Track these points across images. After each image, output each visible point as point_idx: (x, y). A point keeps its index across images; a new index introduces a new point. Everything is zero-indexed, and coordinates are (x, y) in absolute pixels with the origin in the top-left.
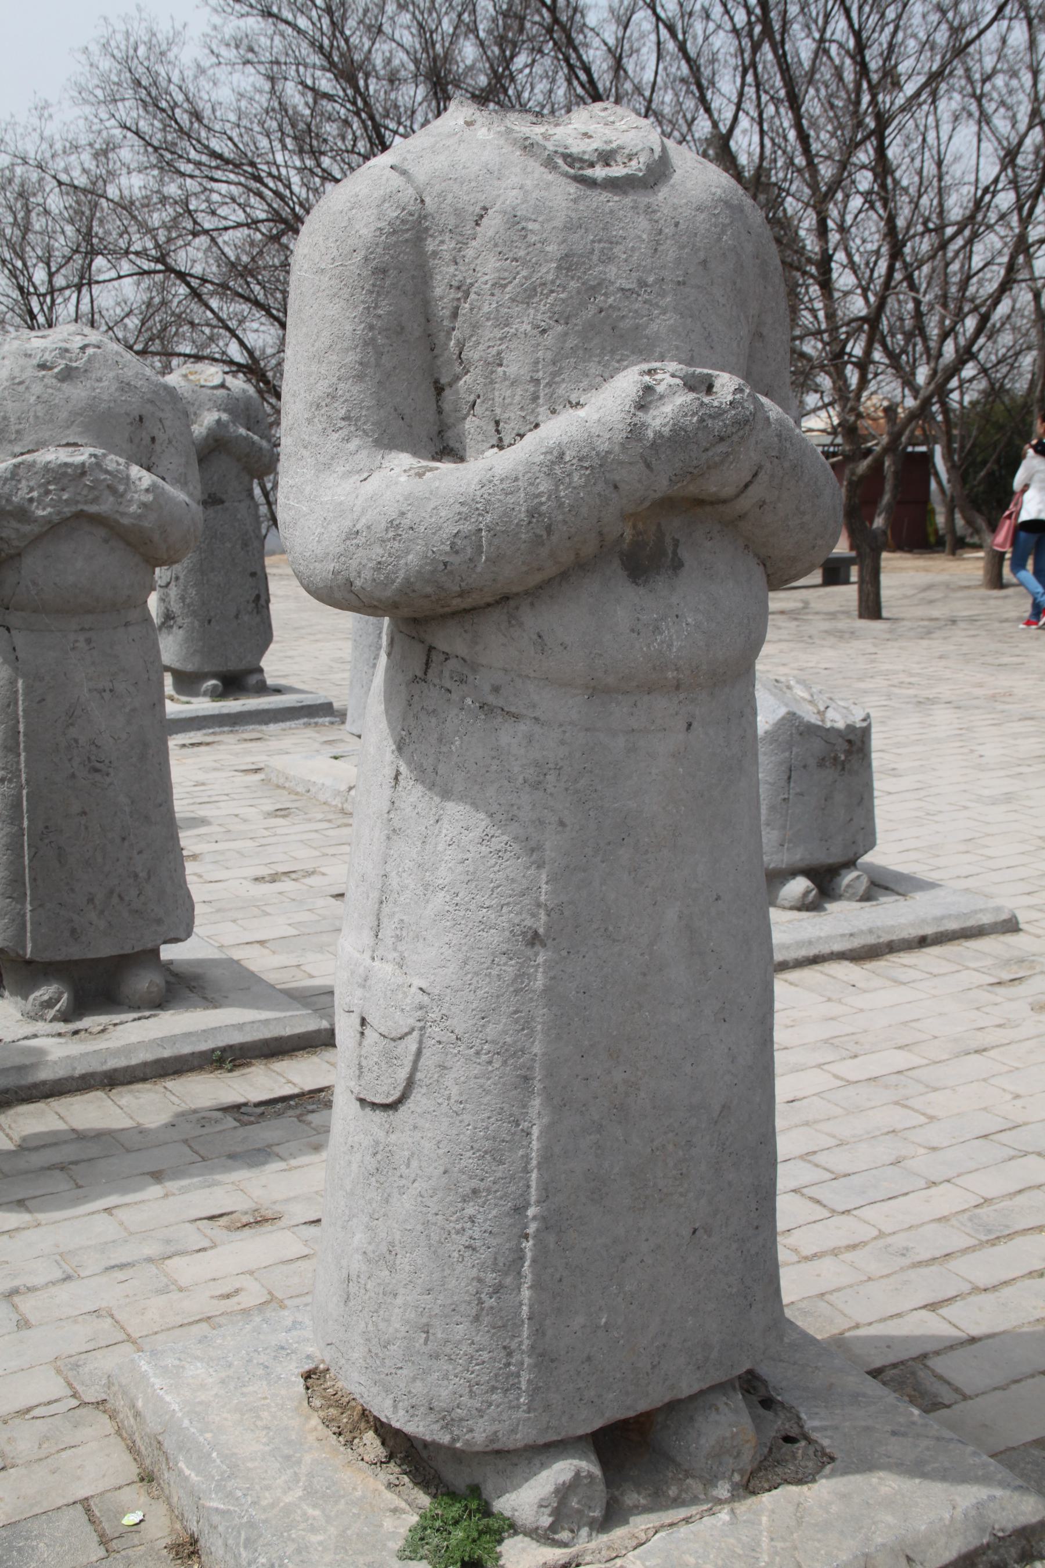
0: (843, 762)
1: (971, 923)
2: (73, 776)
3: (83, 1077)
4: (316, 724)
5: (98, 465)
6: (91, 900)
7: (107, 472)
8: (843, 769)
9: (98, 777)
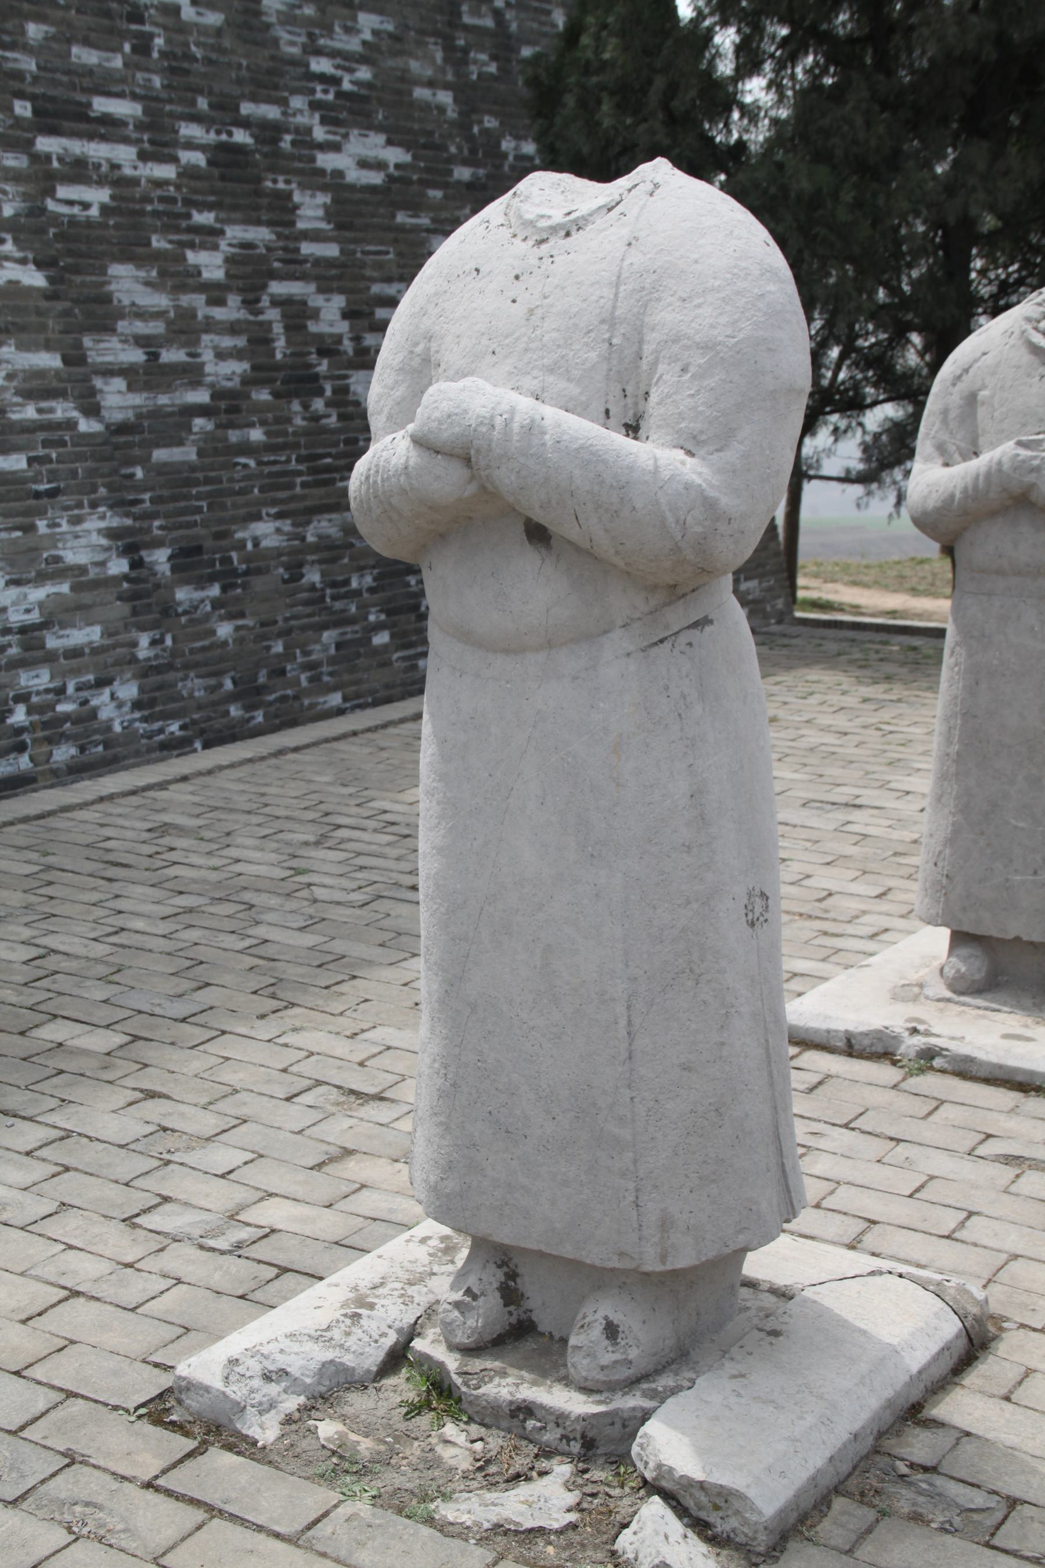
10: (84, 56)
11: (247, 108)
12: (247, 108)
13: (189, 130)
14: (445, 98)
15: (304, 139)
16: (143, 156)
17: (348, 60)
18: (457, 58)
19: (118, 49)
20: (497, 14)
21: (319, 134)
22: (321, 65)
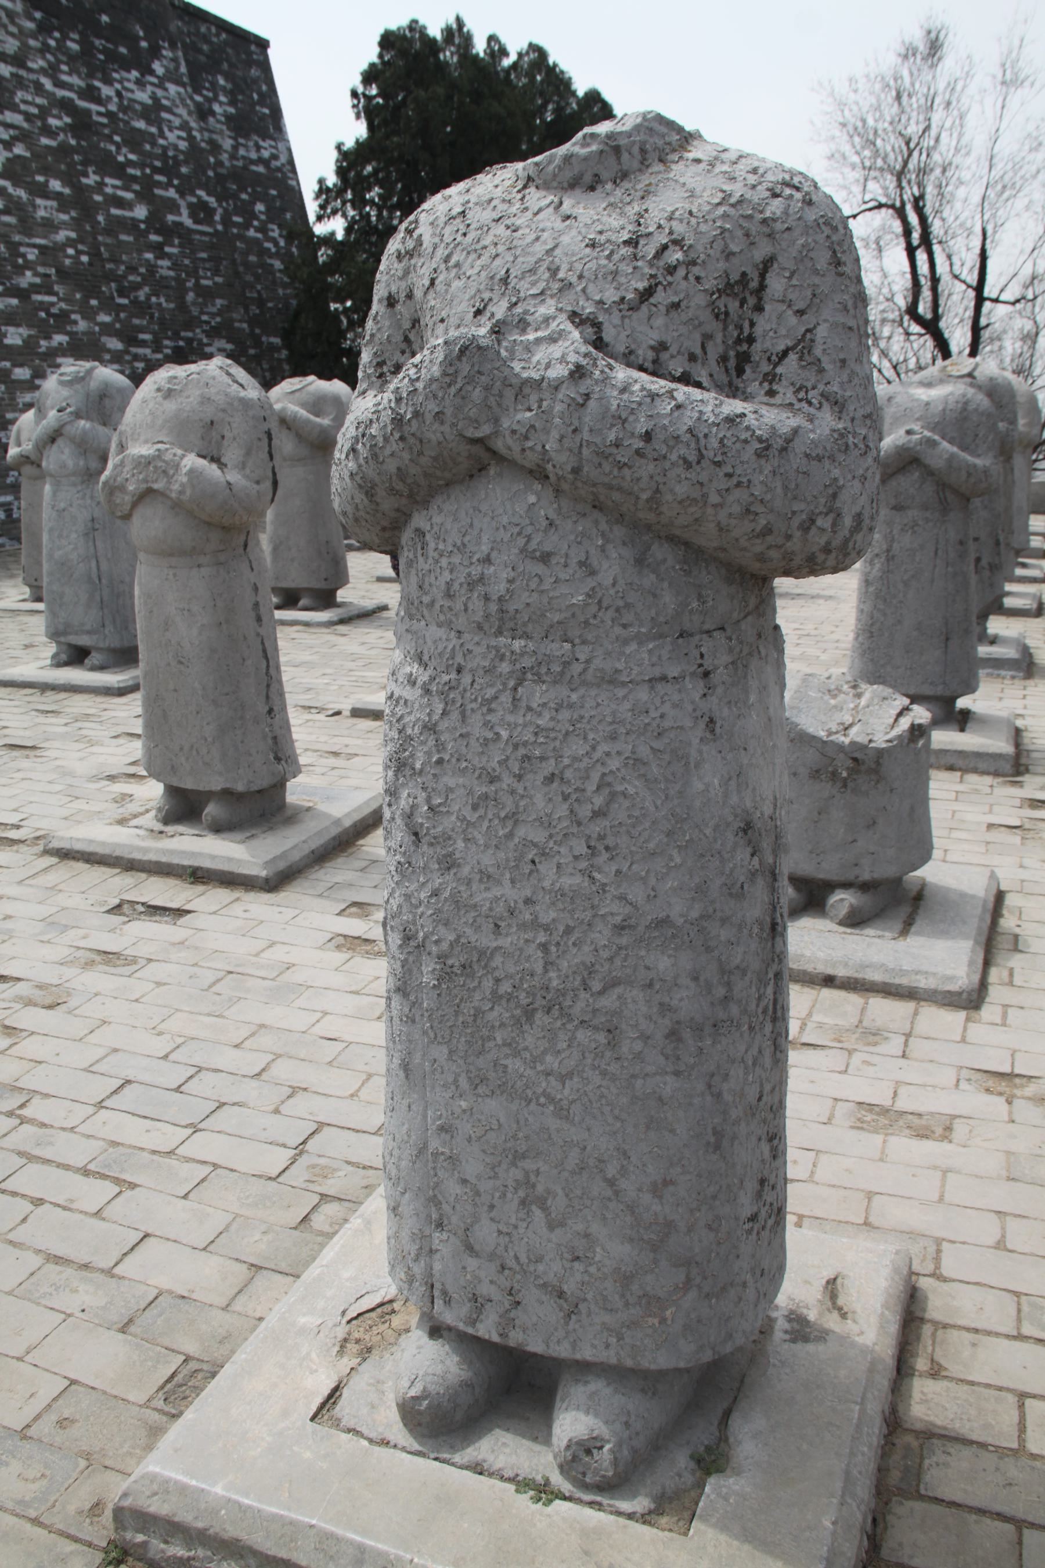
0: (845, 780)
1: (904, 981)
2: (169, 664)
3: (117, 858)
4: (998, 676)
5: (159, 456)
6: (181, 749)
7: (164, 461)
8: (845, 786)
9: (182, 667)
10: (136, 321)
11: (183, 334)
12: (183, 334)
13: (167, 342)
14: (245, 326)
15: (201, 344)
16: (154, 352)
17: (213, 315)
18: (246, 309)
19: (144, 318)
20: (259, 292)
21: (205, 340)
22: (205, 318)
